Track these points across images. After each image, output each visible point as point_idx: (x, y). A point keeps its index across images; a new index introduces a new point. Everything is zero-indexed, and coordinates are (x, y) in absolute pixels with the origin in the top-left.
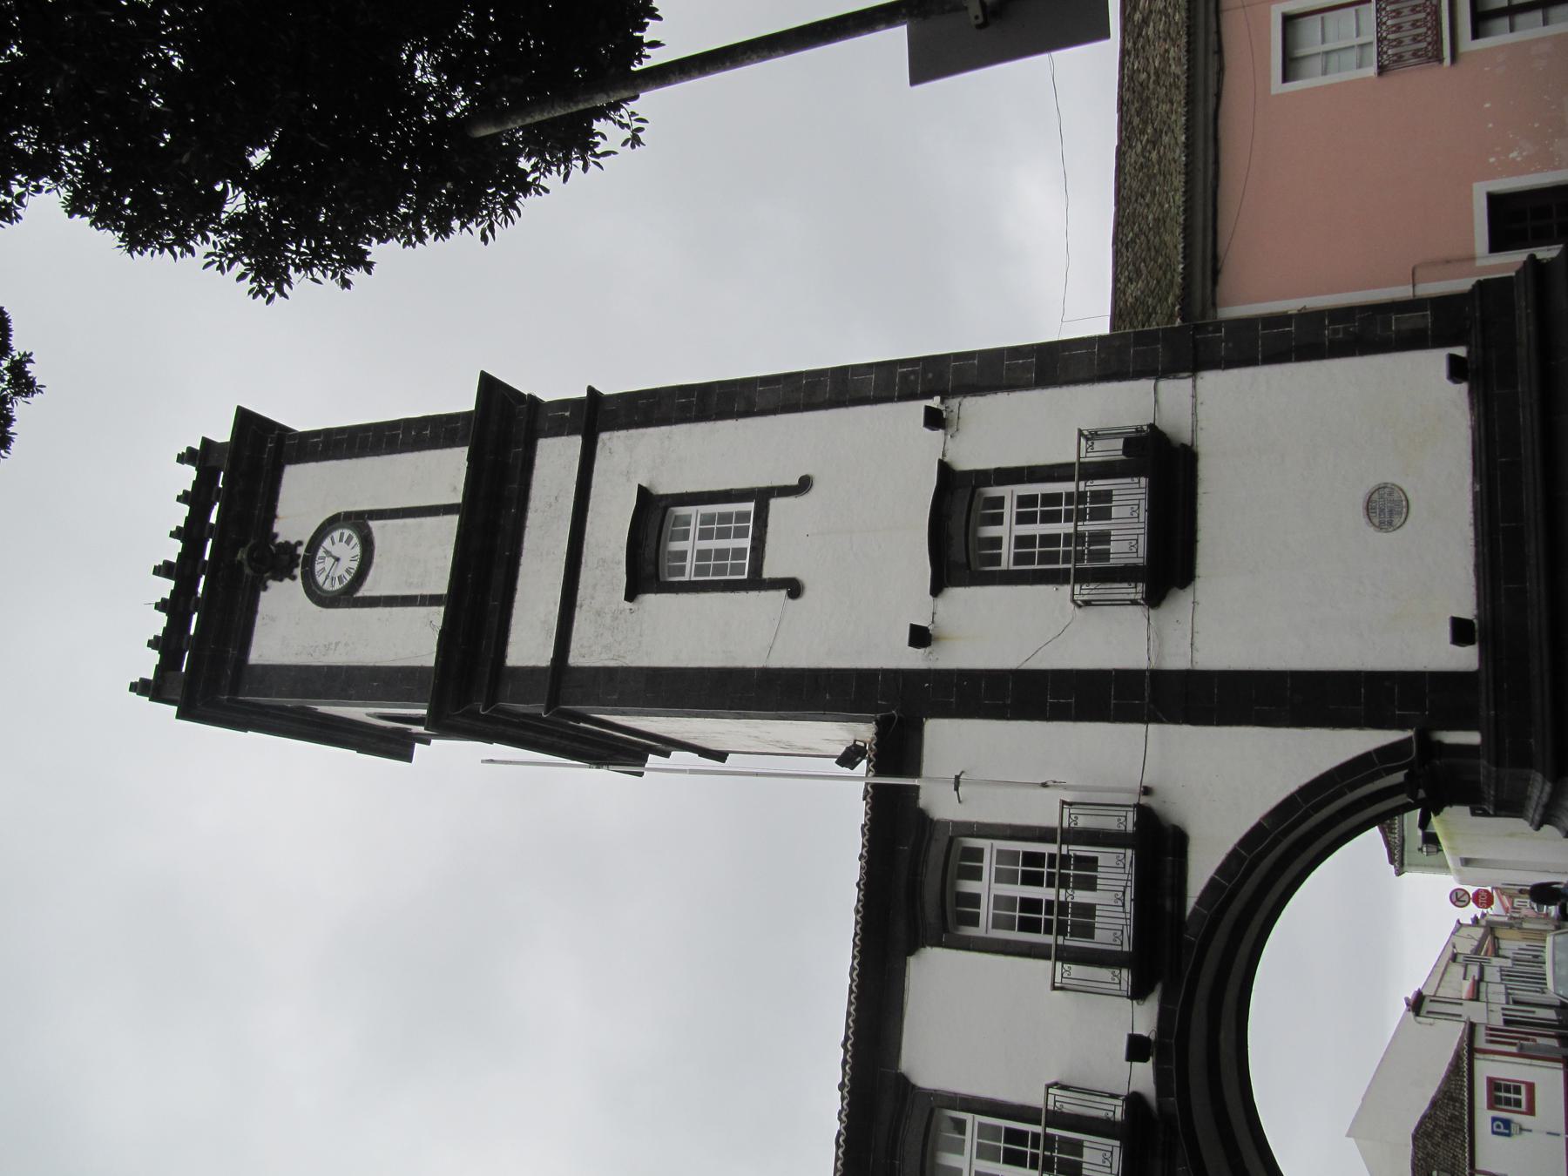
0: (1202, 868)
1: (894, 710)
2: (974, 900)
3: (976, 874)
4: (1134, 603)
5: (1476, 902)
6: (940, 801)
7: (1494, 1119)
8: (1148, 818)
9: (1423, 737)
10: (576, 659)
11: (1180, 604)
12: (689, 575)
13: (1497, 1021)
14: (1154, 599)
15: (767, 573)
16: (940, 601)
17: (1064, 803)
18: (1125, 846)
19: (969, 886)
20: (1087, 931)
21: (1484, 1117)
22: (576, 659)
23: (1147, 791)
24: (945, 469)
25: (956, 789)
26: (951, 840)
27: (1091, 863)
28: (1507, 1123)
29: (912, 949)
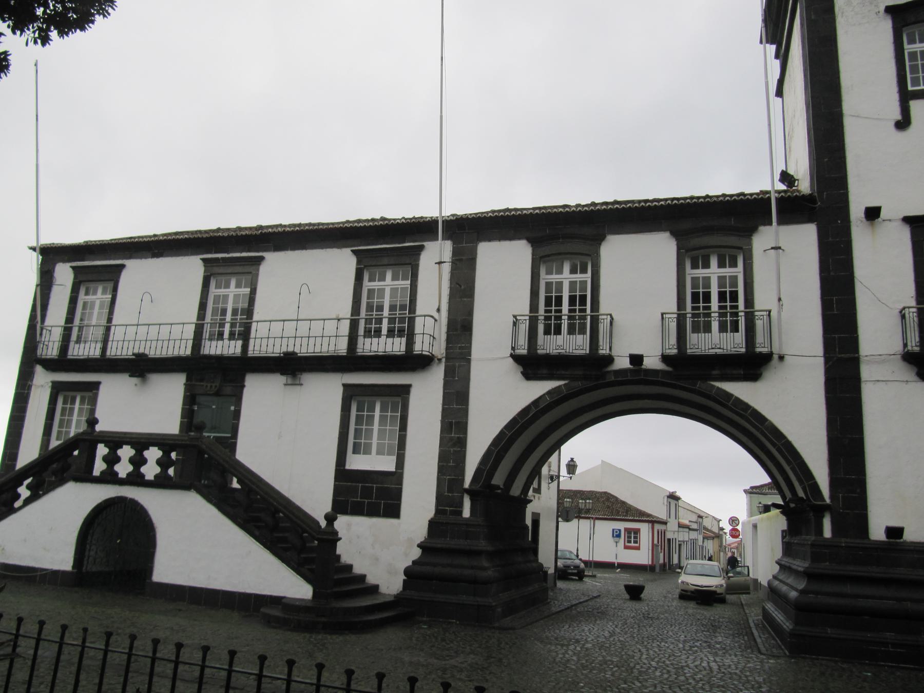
0: (739, 390)
1: (821, 202)
2: (707, 265)
3: (721, 265)
4: (905, 345)
5: (732, 530)
6: (763, 239)
7: (620, 530)
8: (766, 358)
9: (827, 508)
11: (907, 373)
12: (908, 48)
13: (669, 535)
16: (900, 223)
17: (770, 311)
18: (747, 347)
19: (714, 262)
20: (696, 329)
21: (621, 526)
23: (781, 358)
25: (772, 248)
26: (740, 248)
27: (735, 329)
28: (619, 536)
29: (674, 234)
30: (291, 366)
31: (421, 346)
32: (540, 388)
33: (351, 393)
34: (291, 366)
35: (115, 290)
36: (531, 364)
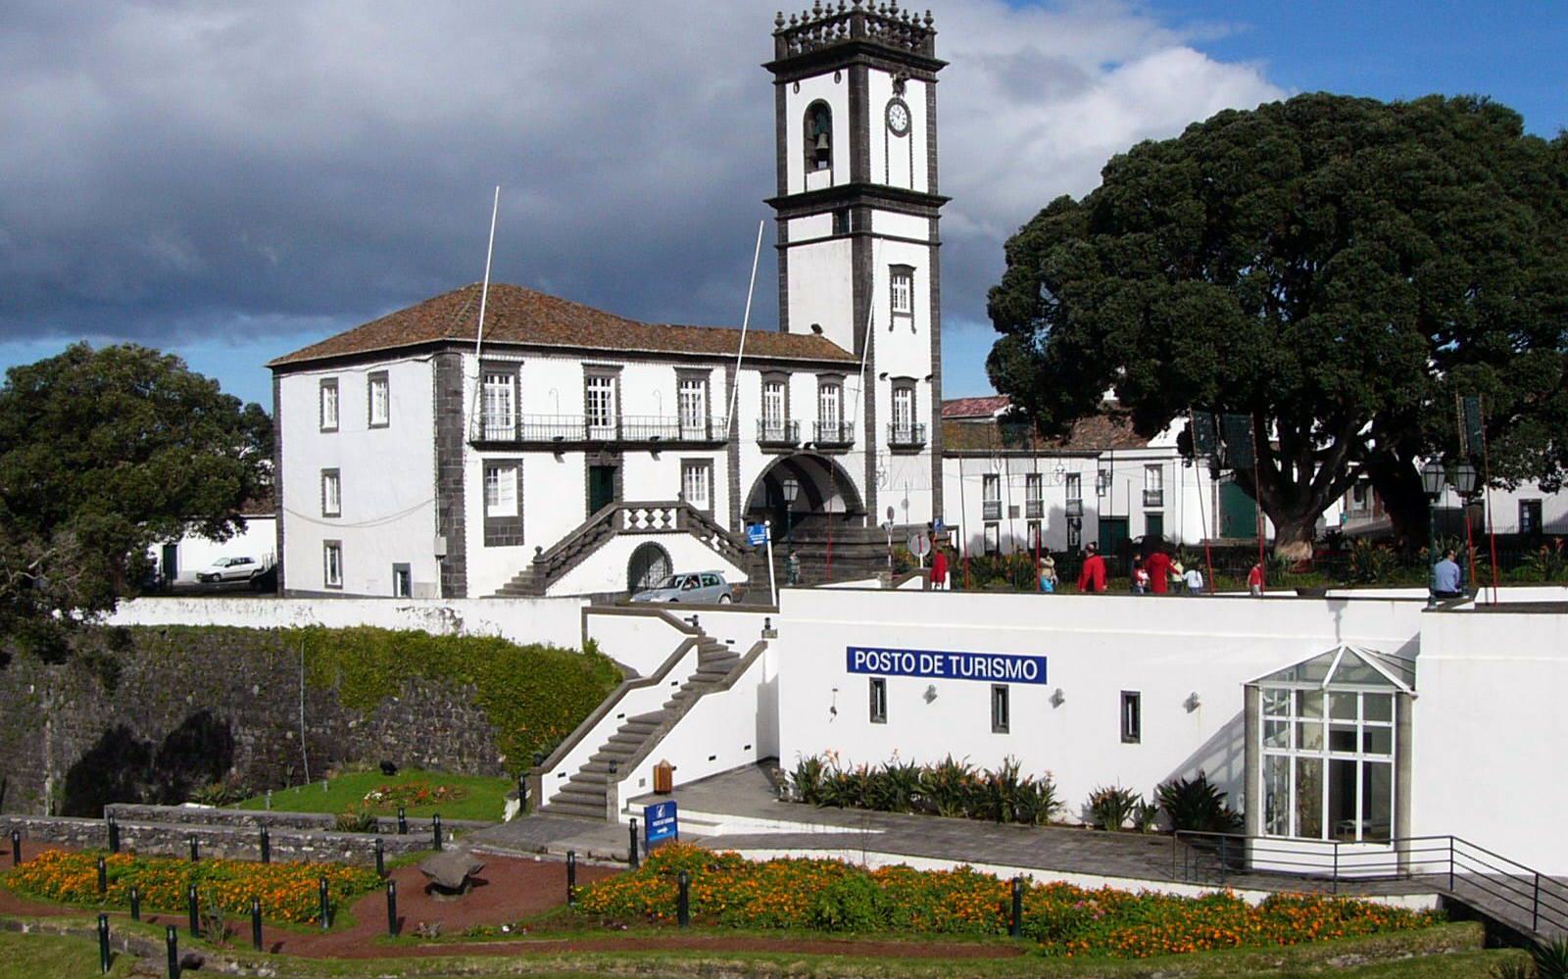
0: (839, 459)
10: (875, 241)
14: (889, 445)
15: (896, 319)
22: (875, 241)
24: (916, 380)
30: (655, 446)
31: (718, 435)
32: (772, 457)
33: (687, 465)
34: (655, 446)
35: (517, 382)
36: (766, 446)
